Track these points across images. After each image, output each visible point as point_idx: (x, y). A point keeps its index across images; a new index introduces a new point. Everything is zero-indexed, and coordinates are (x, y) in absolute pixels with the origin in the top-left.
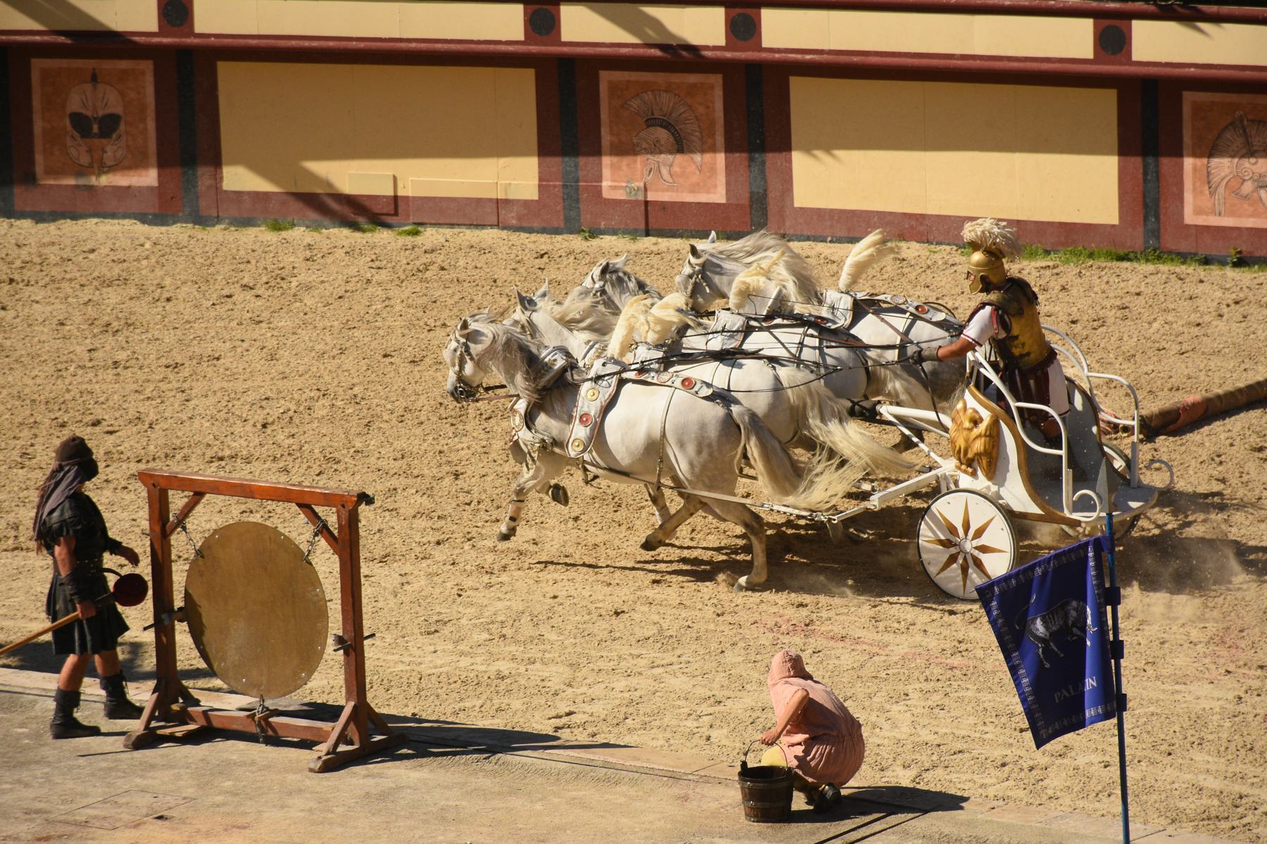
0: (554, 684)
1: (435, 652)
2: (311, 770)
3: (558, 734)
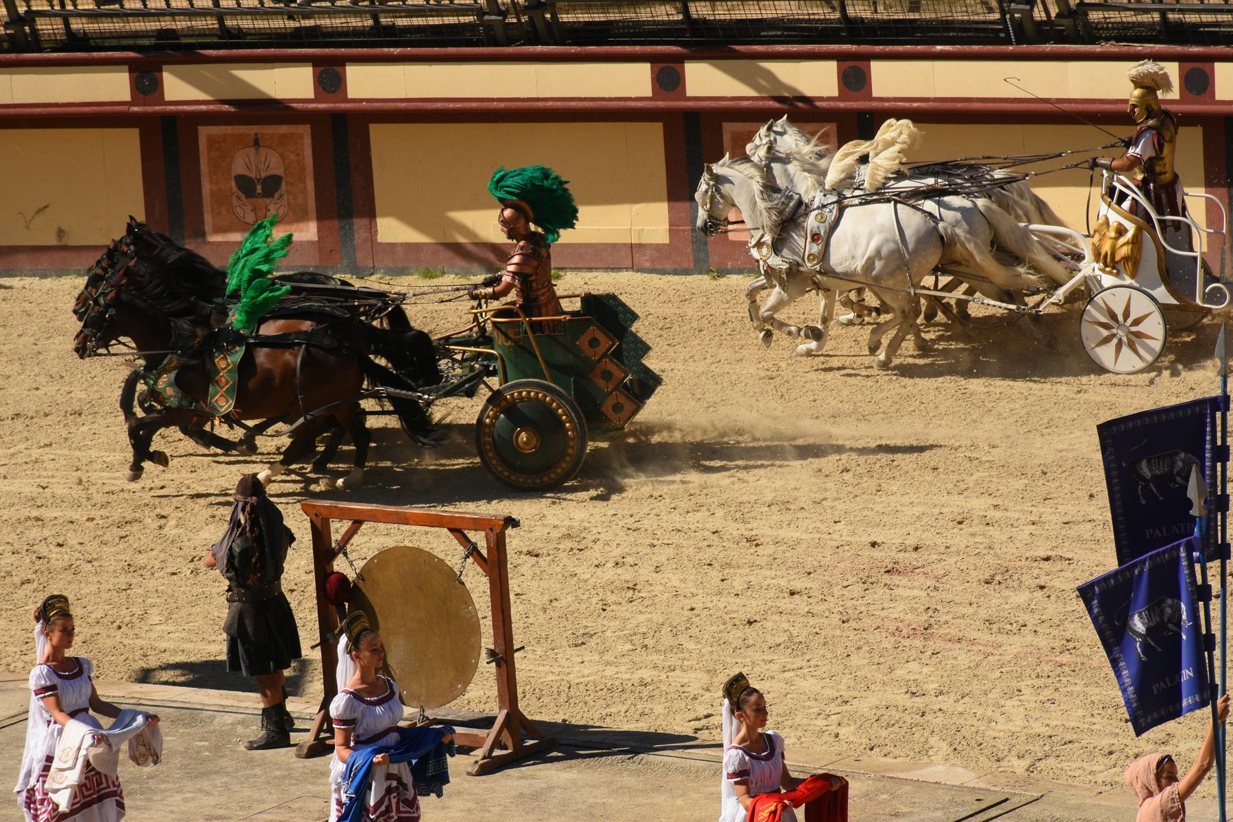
0: (694, 689)
1: (583, 662)
2: (469, 774)
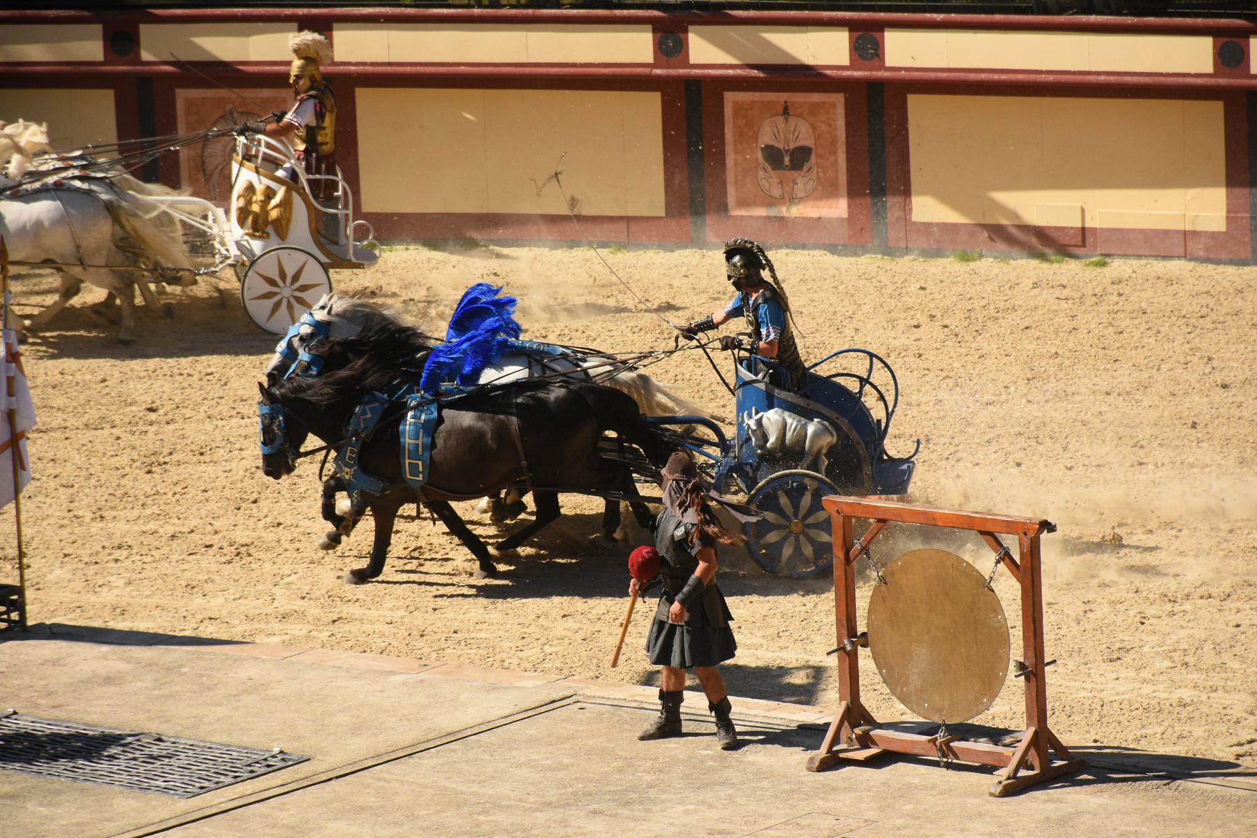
0: (1237, 712)
1: (1117, 679)
2: (992, 795)
3: (1239, 762)
